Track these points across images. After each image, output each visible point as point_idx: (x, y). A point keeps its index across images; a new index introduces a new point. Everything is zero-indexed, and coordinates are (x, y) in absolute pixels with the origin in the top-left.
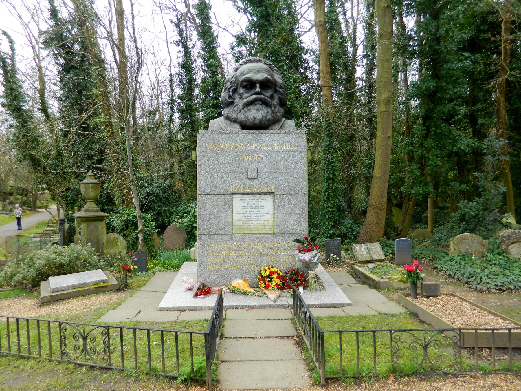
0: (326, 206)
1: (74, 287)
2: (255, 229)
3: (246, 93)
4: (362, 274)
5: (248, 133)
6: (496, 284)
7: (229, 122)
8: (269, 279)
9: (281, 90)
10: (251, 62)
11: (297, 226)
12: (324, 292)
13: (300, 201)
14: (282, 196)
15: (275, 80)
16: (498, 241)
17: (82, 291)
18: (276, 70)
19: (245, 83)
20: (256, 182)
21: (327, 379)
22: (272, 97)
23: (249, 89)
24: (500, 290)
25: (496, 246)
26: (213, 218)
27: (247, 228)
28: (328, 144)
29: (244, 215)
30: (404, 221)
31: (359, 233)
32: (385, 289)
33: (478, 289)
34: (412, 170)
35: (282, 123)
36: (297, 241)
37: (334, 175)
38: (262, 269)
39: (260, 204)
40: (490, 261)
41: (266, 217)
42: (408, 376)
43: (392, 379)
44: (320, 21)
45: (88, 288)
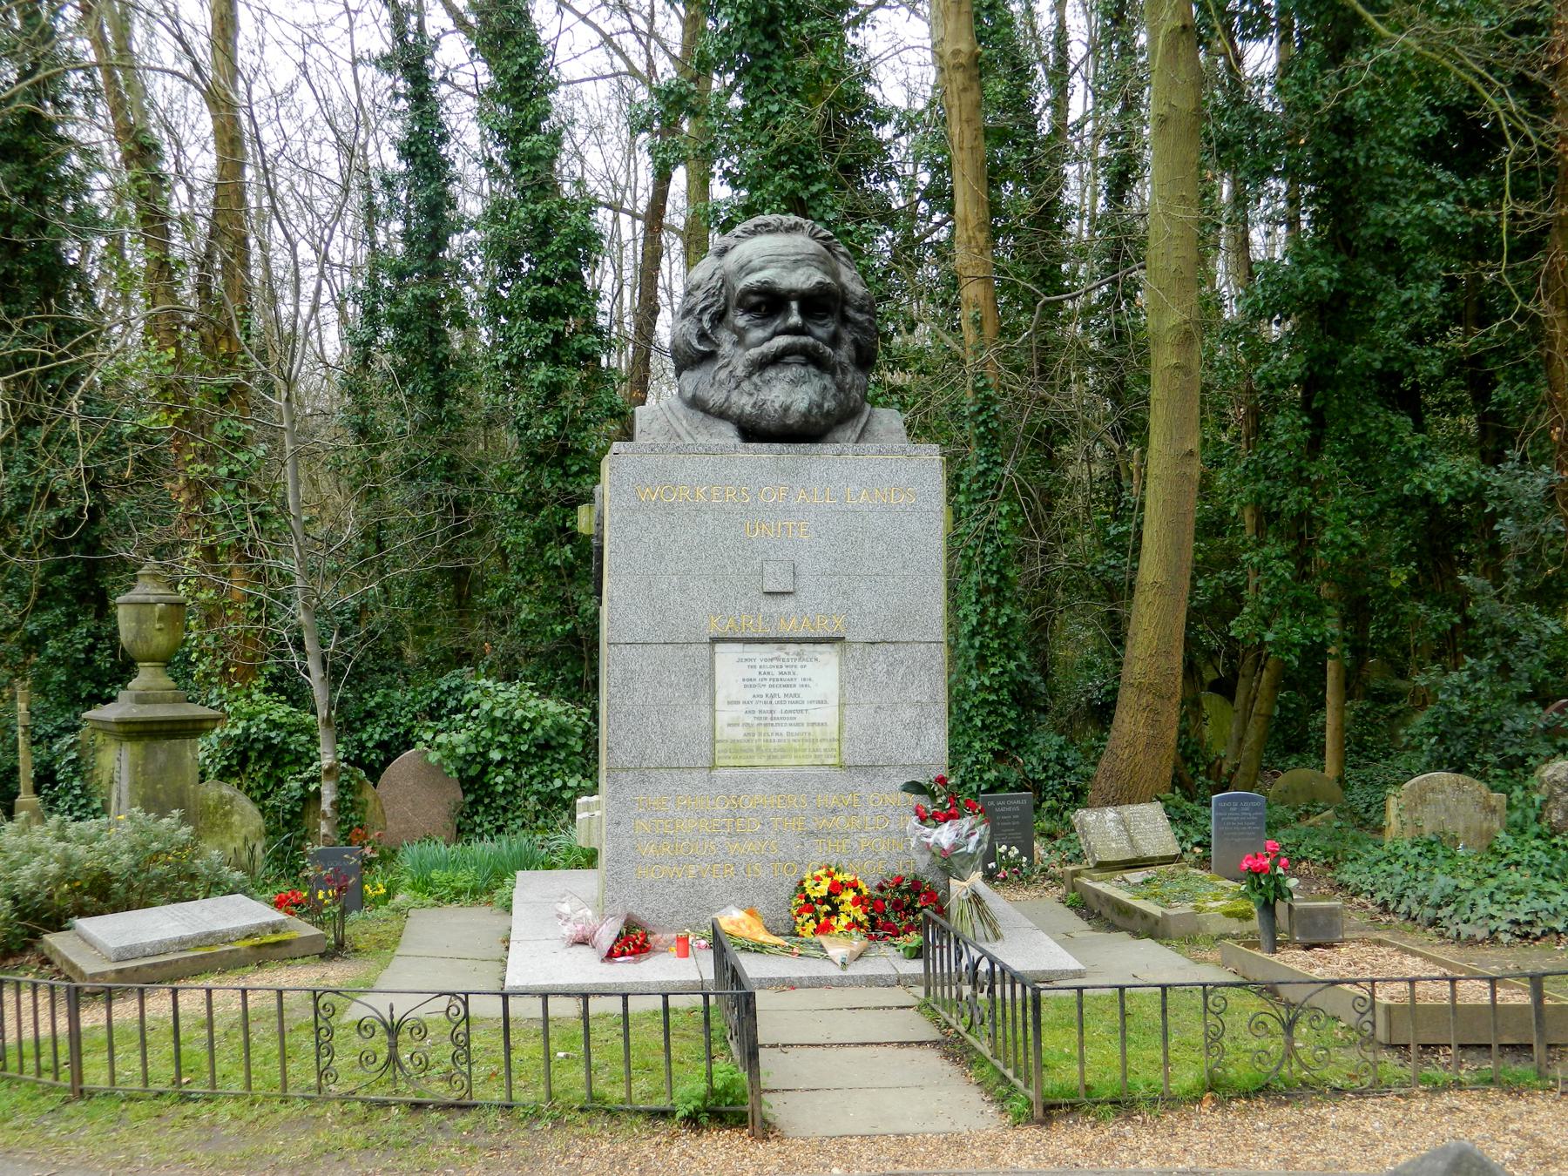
0: (973, 684)
1: (182, 943)
2: (782, 750)
3: (757, 326)
4: (1109, 900)
5: (764, 454)
6: (1513, 917)
7: (701, 415)
8: (827, 908)
9: (860, 317)
10: (769, 232)
11: (914, 742)
12: (998, 944)
13: (924, 665)
14: (868, 648)
15: (843, 287)
16: (1537, 798)
17: (212, 955)
18: (844, 254)
19: (754, 299)
20: (788, 604)
21: (1049, 1108)
22: (834, 341)
23: (763, 317)
24: (1526, 936)
25: (1532, 814)
26: (654, 718)
27: (759, 748)
28: (980, 468)
29: (750, 707)
30: (1241, 740)
31: (1088, 777)
32: (1182, 938)
33: (1463, 937)
34: (1266, 560)
35: (864, 419)
36: (915, 788)
37: (1003, 577)
38: (808, 876)
39: (801, 673)
40: (1504, 855)
41: (818, 715)
42: (1248, 1097)
43: (1208, 1104)
44: (956, 53)
45: (228, 947)
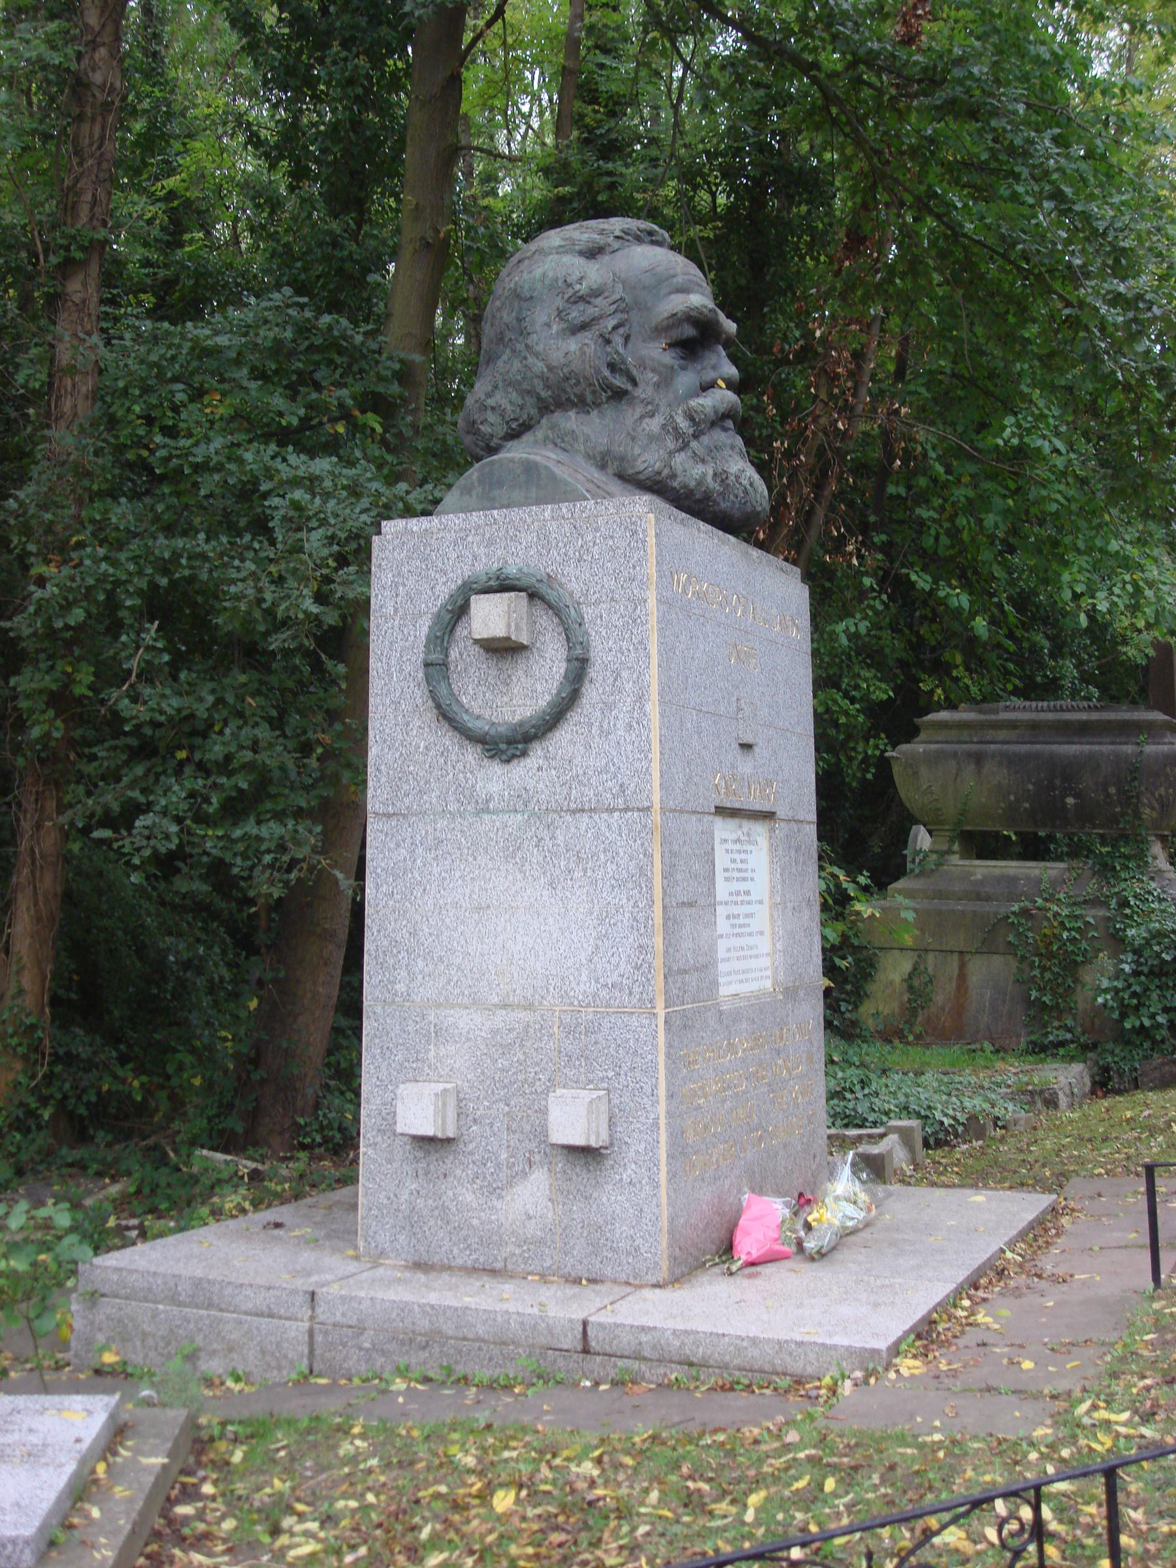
3: (683, 368)
10: (653, 243)
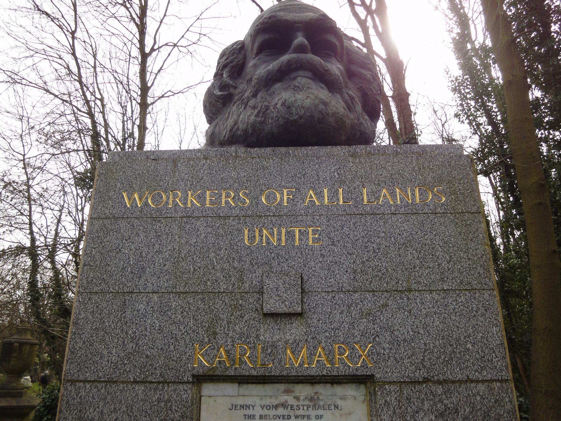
20: (294, 331)
